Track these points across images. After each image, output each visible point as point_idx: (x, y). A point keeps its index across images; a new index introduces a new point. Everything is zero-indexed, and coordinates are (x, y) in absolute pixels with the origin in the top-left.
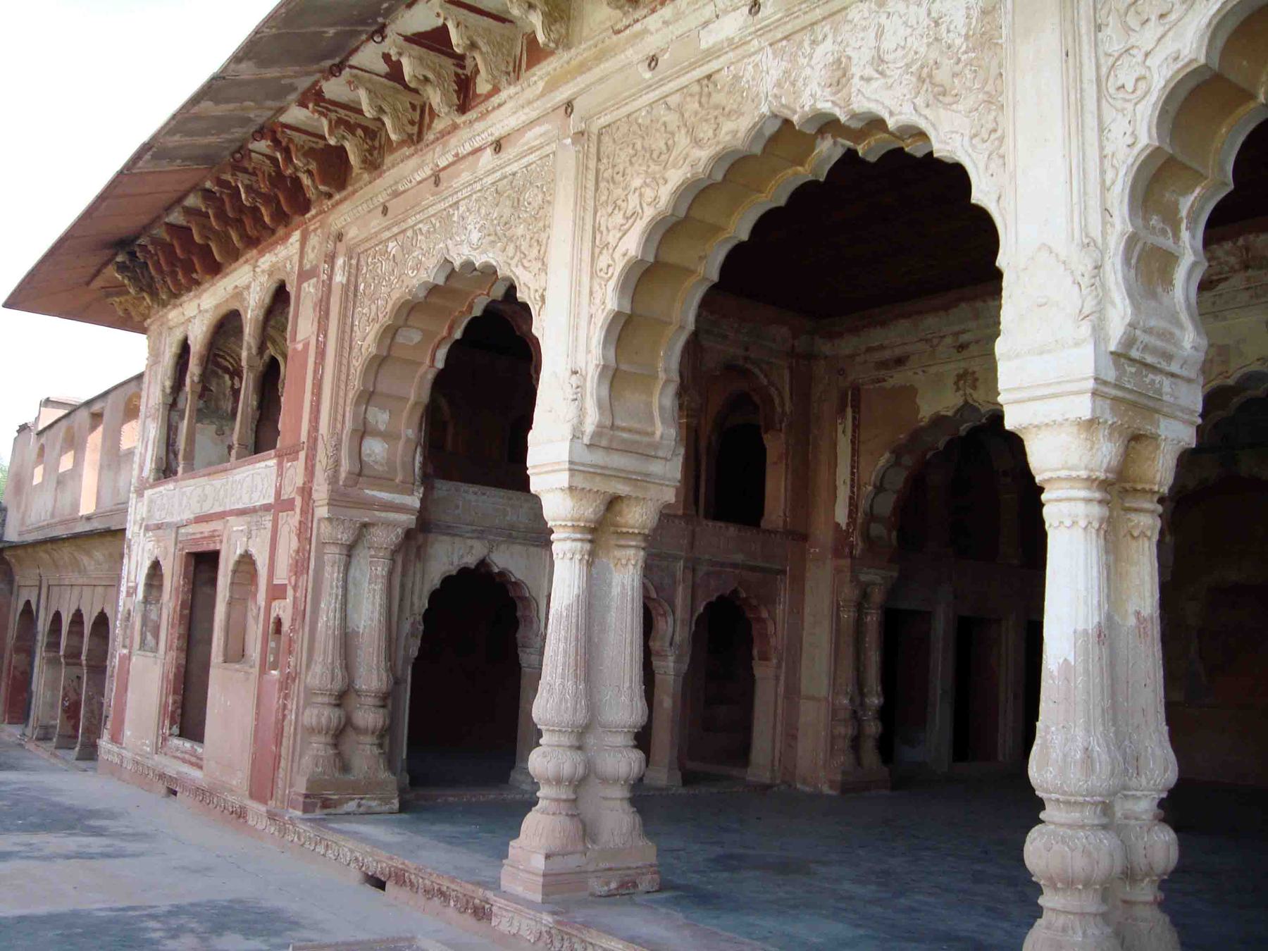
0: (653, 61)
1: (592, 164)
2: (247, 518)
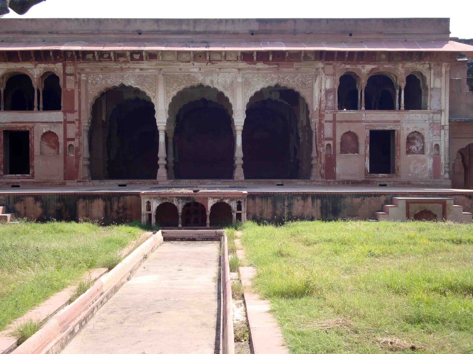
0: (180, 69)
1: (166, 79)
2: (50, 124)
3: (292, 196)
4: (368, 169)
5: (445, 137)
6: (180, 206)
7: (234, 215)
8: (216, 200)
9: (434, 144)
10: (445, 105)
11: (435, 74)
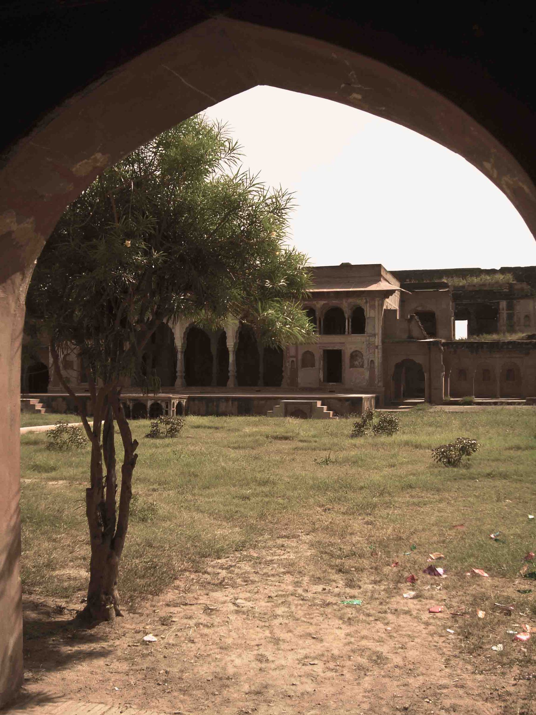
3: (219, 399)
4: (322, 379)
5: (378, 355)
6: (131, 405)
7: (164, 411)
8: (153, 401)
9: (370, 359)
10: (379, 330)
11: (370, 307)
